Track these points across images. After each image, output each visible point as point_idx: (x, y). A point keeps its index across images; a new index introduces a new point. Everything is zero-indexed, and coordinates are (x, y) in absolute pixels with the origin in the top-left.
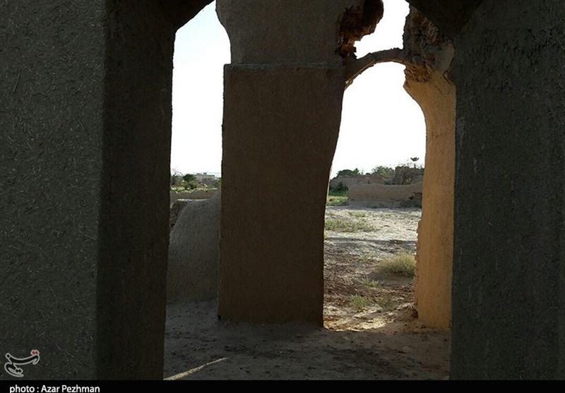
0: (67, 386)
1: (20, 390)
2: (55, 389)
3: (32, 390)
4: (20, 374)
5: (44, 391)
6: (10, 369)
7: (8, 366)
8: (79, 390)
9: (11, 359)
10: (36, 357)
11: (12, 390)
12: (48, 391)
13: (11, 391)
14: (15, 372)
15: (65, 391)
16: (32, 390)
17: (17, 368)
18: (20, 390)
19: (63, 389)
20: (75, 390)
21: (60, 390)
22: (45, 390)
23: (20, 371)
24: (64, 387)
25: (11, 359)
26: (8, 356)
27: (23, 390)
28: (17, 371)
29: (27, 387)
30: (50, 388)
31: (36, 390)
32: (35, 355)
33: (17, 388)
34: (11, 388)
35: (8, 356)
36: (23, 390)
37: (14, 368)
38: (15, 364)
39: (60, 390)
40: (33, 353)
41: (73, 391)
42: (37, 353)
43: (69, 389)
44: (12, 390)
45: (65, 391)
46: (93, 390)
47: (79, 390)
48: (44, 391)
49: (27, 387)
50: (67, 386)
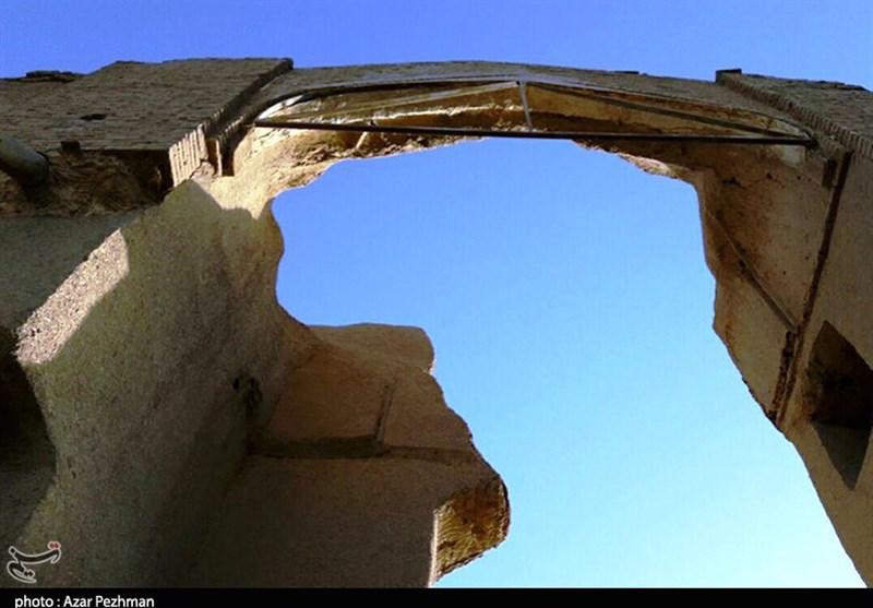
0: (104, 598)
1: (32, 603)
2: (85, 602)
3: (49, 603)
4: (29, 577)
5: (68, 605)
6: (15, 571)
7: (13, 566)
8: (122, 603)
9: (17, 555)
10: (56, 552)
11: (19, 603)
12: (75, 605)
13: (17, 605)
14: (23, 576)
15: (101, 604)
16: (49, 603)
17: (26, 570)
18: (32, 603)
19: (97, 602)
20: (117, 603)
21: (93, 603)
22: (70, 603)
23: (31, 574)
24: (99, 599)
25: (17, 555)
26: (13, 551)
27: (36, 603)
28: (26, 574)
29: (42, 599)
30: (78, 600)
31: (56, 603)
32: (55, 549)
33: (26, 600)
34: (17, 601)
35: (13, 551)
36: (36, 603)
37: (22, 570)
38: (22, 563)
39: (93, 603)
41: (113, 605)
42: (57, 546)
43: (106, 602)
44: (19, 603)
45: (101, 604)
46: (143, 603)
47: (122, 603)
48: (68, 605)
49: (42, 599)
50: (104, 598)
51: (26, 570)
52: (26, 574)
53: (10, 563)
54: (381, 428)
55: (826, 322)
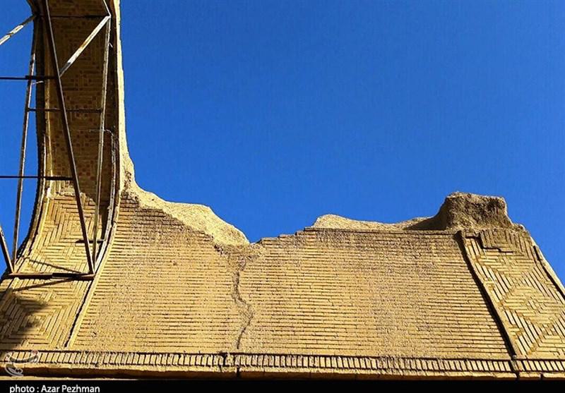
0: (67, 386)
1: (20, 390)
2: (55, 389)
3: (32, 390)
5: (44, 391)
8: (79, 390)
11: (12, 390)
12: (48, 391)
13: (11, 391)
14: (15, 372)
15: (65, 391)
16: (32, 390)
18: (20, 390)
19: (63, 389)
20: (75, 390)
21: (60, 390)
24: (64, 387)
27: (23, 389)
28: (17, 371)
29: (27, 387)
30: (50, 388)
31: (36, 390)
33: (17, 388)
34: (11, 388)
36: (23, 389)
39: (60, 390)
41: (73, 391)
43: (69, 389)
44: (12, 390)
45: (65, 391)
46: (93, 390)
47: (79, 390)
48: (44, 391)
49: (27, 387)
50: (67, 386)
54: (77, 312)
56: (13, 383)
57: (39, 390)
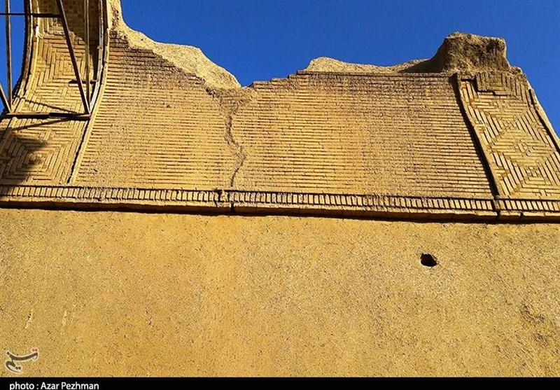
0: (67, 383)
1: (20, 387)
2: (55, 386)
3: (32, 387)
4: (19, 370)
5: (44, 388)
6: (10, 366)
7: (8, 363)
8: (78, 387)
9: (11, 356)
10: (36, 354)
11: (12, 387)
12: (48, 388)
13: (11, 388)
14: (16, 370)
15: (65, 388)
16: (32, 387)
17: (16, 366)
18: (20, 387)
19: (63, 386)
20: (75, 387)
21: (60, 387)
22: (45, 387)
23: (20, 368)
24: (63, 384)
25: (11, 356)
26: (8, 353)
27: (23, 387)
28: (17, 368)
29: (27, 384)
30: (50, 385)
31: (36, 387)
32: (35, 352)
33: (16, 385)
34: (11, 385)
35: (8, 353)
36: (23, 387)
37: (14, 365)
38: (15, 362)
39: (60, 387)
40: (33, 350)
41: (72, 388)
42: (36, 350)
43: (68, 386)
44: (12, 387)
45: (65, 388)
46: (92, 387)
47: (78, 387)
48: (44, 388)
49: (27, 384)
50: (67, 383)
51: (16, 366)
52: (17, 368)
53: (6, 361)
55: (423, 255)
56: (13, 380)
57: (39, 387)
